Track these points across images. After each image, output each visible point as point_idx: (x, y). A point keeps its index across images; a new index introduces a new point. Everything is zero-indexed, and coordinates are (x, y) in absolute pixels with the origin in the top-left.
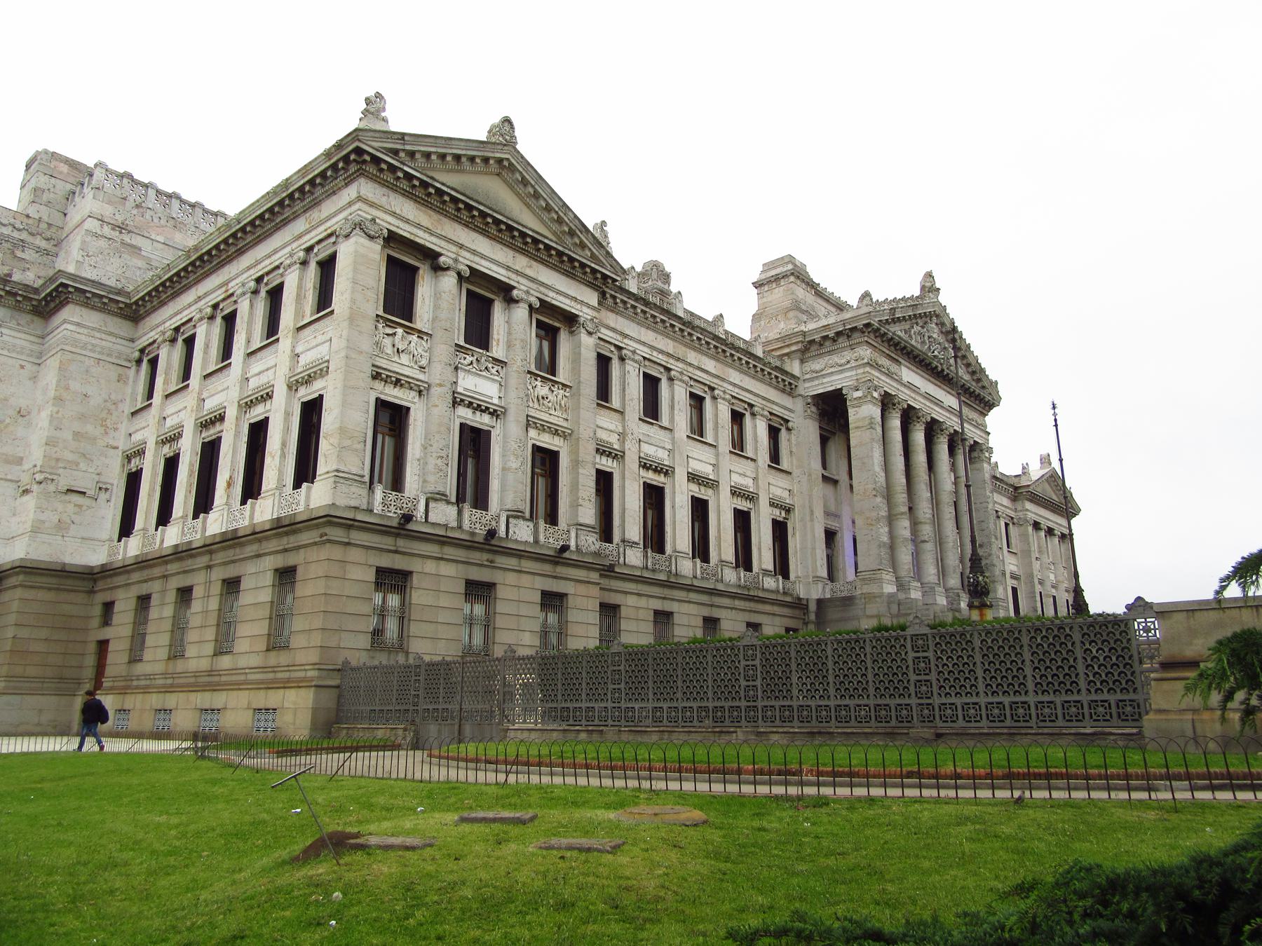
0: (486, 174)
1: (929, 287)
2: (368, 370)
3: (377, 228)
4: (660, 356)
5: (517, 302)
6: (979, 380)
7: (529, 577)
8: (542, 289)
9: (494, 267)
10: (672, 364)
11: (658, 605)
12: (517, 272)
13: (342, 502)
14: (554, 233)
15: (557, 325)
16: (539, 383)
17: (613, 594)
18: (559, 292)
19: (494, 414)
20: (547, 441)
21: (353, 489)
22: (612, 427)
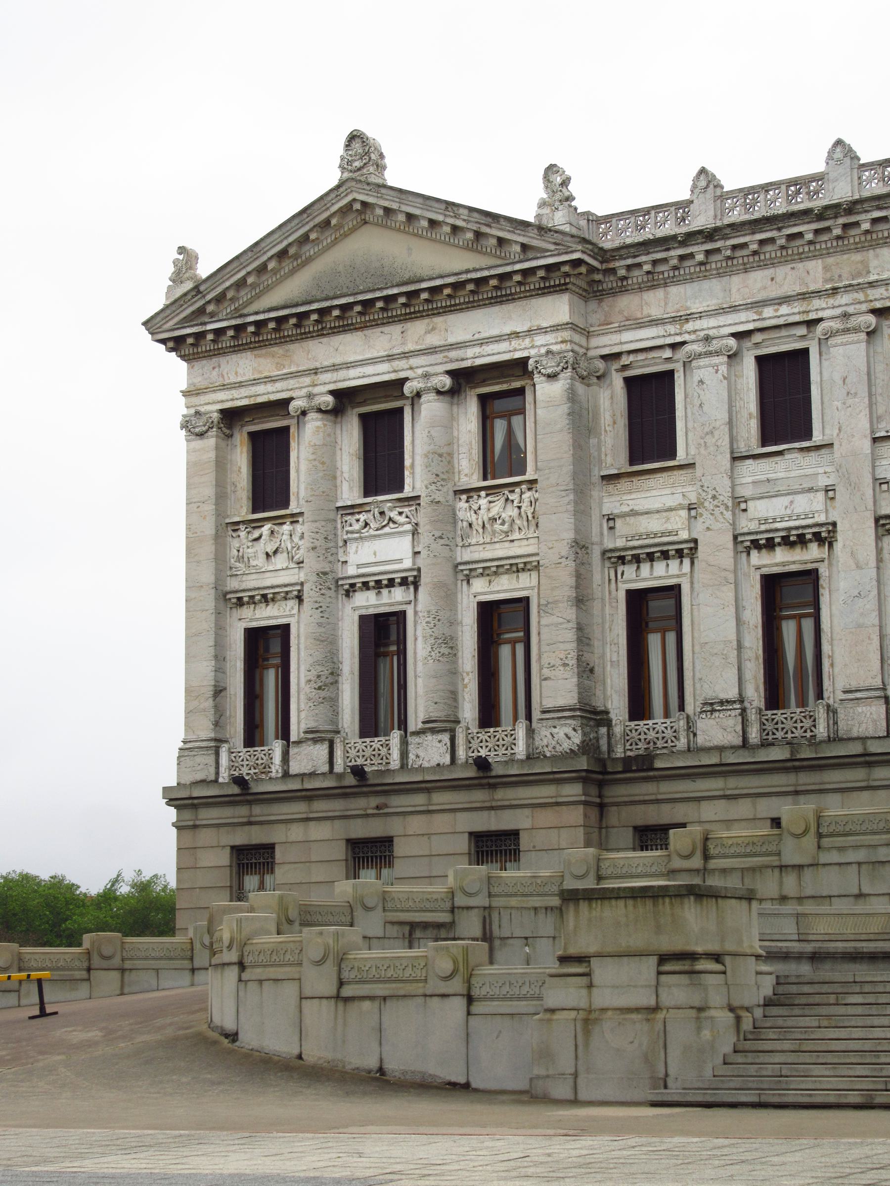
0: (346, 235)
2: (209, 601)
3: (204, 419)
4: (784, 309)
5: (418, 395)
7: (447, 817)
8: (453, 354)
9: (369, 370)
10: (820, 308)
12: (406, 355)
13: (188, 779)
14: (467, 248)
15: (517, 384)
16: (483, 502)
17: (666, 807)
18: (482, 342)
19: (404, 582)
20: (504, 588)
21: (199, 759)
22: (670, 502)
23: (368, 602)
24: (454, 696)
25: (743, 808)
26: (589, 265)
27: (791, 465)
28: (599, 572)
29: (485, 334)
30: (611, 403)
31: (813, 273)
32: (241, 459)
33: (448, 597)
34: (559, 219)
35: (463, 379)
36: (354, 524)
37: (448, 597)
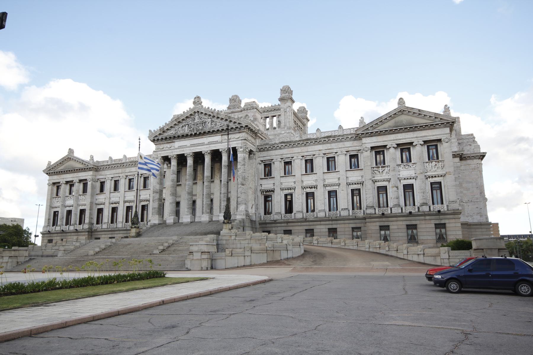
6: (231, 121)
10: (121, 175)
11: (110, 236)
16: (82, 196)
23: (68, 209)
24: (76, 221)
25: (106, 236)
26: (96, 168)
27: (116, 194)
28: (94, 206)
29: (83, 175)
30: (98, 185)
31: (120, 171)
32: (55, 188)
33: (76, 208)
34: (91, 162)
35: (80, 181)
36: (67, 198)
37: (76, 208)
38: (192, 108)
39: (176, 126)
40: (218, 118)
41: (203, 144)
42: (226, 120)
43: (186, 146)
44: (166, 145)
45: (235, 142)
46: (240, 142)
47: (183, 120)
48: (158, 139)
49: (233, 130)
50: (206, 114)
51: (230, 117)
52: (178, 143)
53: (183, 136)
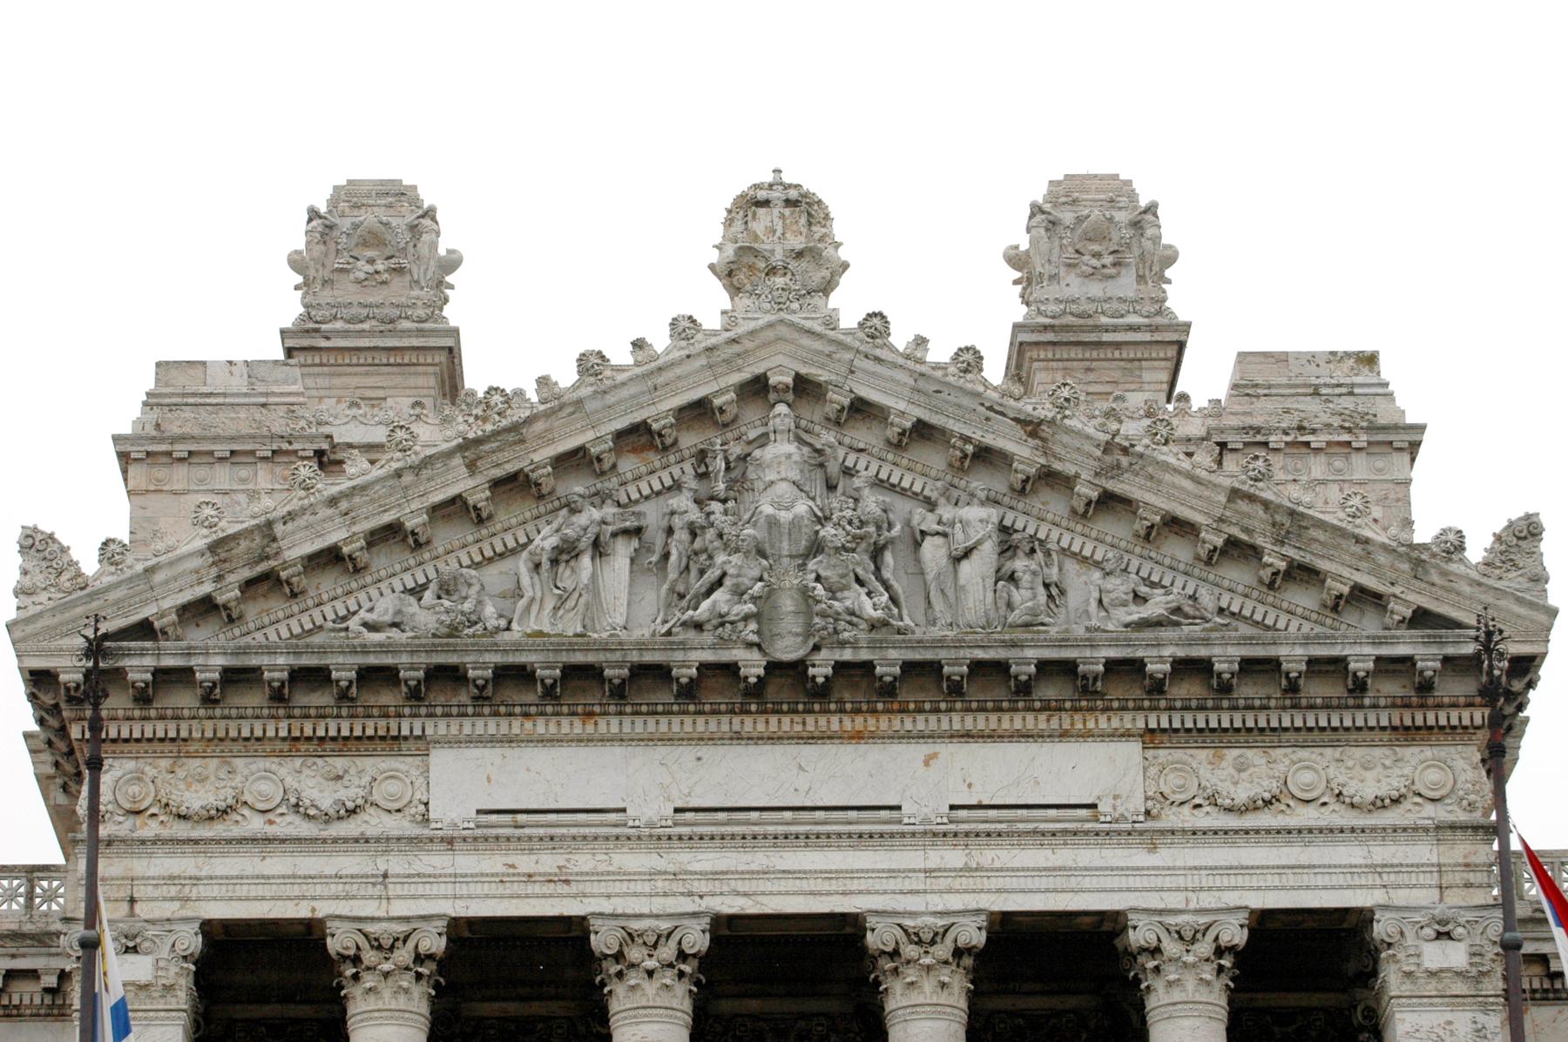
1: (778, 239)
6: (1302, 573)
38: (711, 320)
39: (447, 536)
40: (1109, 502)
41: (873, 823)
42: (1238, 550)
43: (603, 825)
44: (264, 779)
45: (1349, 853)
46: (1424, 852)
47: (575, 460)
48: (165, 677)
49: (1316, 690)
50: (923, 431)
51: (1294, 523)
52: (466, 774)
53: (580, 676)
